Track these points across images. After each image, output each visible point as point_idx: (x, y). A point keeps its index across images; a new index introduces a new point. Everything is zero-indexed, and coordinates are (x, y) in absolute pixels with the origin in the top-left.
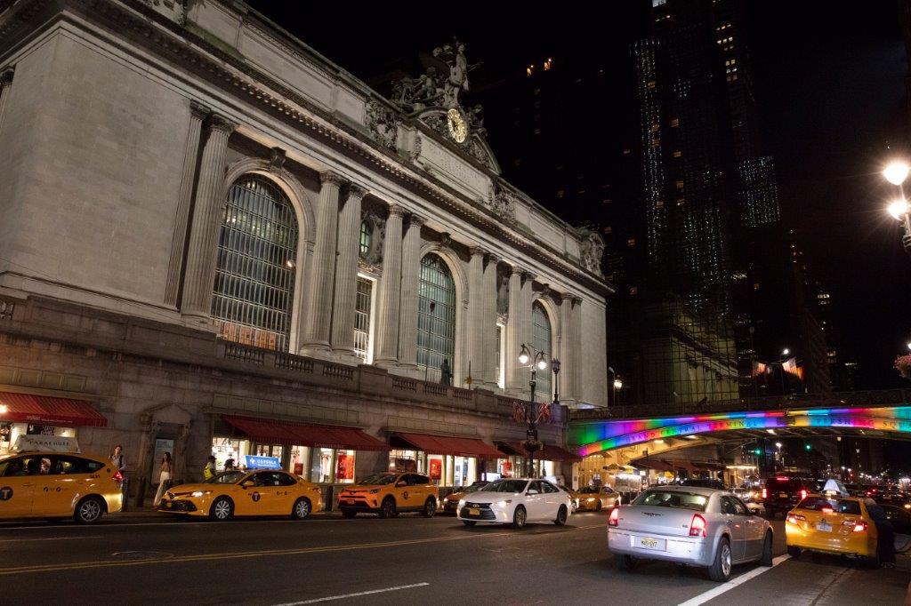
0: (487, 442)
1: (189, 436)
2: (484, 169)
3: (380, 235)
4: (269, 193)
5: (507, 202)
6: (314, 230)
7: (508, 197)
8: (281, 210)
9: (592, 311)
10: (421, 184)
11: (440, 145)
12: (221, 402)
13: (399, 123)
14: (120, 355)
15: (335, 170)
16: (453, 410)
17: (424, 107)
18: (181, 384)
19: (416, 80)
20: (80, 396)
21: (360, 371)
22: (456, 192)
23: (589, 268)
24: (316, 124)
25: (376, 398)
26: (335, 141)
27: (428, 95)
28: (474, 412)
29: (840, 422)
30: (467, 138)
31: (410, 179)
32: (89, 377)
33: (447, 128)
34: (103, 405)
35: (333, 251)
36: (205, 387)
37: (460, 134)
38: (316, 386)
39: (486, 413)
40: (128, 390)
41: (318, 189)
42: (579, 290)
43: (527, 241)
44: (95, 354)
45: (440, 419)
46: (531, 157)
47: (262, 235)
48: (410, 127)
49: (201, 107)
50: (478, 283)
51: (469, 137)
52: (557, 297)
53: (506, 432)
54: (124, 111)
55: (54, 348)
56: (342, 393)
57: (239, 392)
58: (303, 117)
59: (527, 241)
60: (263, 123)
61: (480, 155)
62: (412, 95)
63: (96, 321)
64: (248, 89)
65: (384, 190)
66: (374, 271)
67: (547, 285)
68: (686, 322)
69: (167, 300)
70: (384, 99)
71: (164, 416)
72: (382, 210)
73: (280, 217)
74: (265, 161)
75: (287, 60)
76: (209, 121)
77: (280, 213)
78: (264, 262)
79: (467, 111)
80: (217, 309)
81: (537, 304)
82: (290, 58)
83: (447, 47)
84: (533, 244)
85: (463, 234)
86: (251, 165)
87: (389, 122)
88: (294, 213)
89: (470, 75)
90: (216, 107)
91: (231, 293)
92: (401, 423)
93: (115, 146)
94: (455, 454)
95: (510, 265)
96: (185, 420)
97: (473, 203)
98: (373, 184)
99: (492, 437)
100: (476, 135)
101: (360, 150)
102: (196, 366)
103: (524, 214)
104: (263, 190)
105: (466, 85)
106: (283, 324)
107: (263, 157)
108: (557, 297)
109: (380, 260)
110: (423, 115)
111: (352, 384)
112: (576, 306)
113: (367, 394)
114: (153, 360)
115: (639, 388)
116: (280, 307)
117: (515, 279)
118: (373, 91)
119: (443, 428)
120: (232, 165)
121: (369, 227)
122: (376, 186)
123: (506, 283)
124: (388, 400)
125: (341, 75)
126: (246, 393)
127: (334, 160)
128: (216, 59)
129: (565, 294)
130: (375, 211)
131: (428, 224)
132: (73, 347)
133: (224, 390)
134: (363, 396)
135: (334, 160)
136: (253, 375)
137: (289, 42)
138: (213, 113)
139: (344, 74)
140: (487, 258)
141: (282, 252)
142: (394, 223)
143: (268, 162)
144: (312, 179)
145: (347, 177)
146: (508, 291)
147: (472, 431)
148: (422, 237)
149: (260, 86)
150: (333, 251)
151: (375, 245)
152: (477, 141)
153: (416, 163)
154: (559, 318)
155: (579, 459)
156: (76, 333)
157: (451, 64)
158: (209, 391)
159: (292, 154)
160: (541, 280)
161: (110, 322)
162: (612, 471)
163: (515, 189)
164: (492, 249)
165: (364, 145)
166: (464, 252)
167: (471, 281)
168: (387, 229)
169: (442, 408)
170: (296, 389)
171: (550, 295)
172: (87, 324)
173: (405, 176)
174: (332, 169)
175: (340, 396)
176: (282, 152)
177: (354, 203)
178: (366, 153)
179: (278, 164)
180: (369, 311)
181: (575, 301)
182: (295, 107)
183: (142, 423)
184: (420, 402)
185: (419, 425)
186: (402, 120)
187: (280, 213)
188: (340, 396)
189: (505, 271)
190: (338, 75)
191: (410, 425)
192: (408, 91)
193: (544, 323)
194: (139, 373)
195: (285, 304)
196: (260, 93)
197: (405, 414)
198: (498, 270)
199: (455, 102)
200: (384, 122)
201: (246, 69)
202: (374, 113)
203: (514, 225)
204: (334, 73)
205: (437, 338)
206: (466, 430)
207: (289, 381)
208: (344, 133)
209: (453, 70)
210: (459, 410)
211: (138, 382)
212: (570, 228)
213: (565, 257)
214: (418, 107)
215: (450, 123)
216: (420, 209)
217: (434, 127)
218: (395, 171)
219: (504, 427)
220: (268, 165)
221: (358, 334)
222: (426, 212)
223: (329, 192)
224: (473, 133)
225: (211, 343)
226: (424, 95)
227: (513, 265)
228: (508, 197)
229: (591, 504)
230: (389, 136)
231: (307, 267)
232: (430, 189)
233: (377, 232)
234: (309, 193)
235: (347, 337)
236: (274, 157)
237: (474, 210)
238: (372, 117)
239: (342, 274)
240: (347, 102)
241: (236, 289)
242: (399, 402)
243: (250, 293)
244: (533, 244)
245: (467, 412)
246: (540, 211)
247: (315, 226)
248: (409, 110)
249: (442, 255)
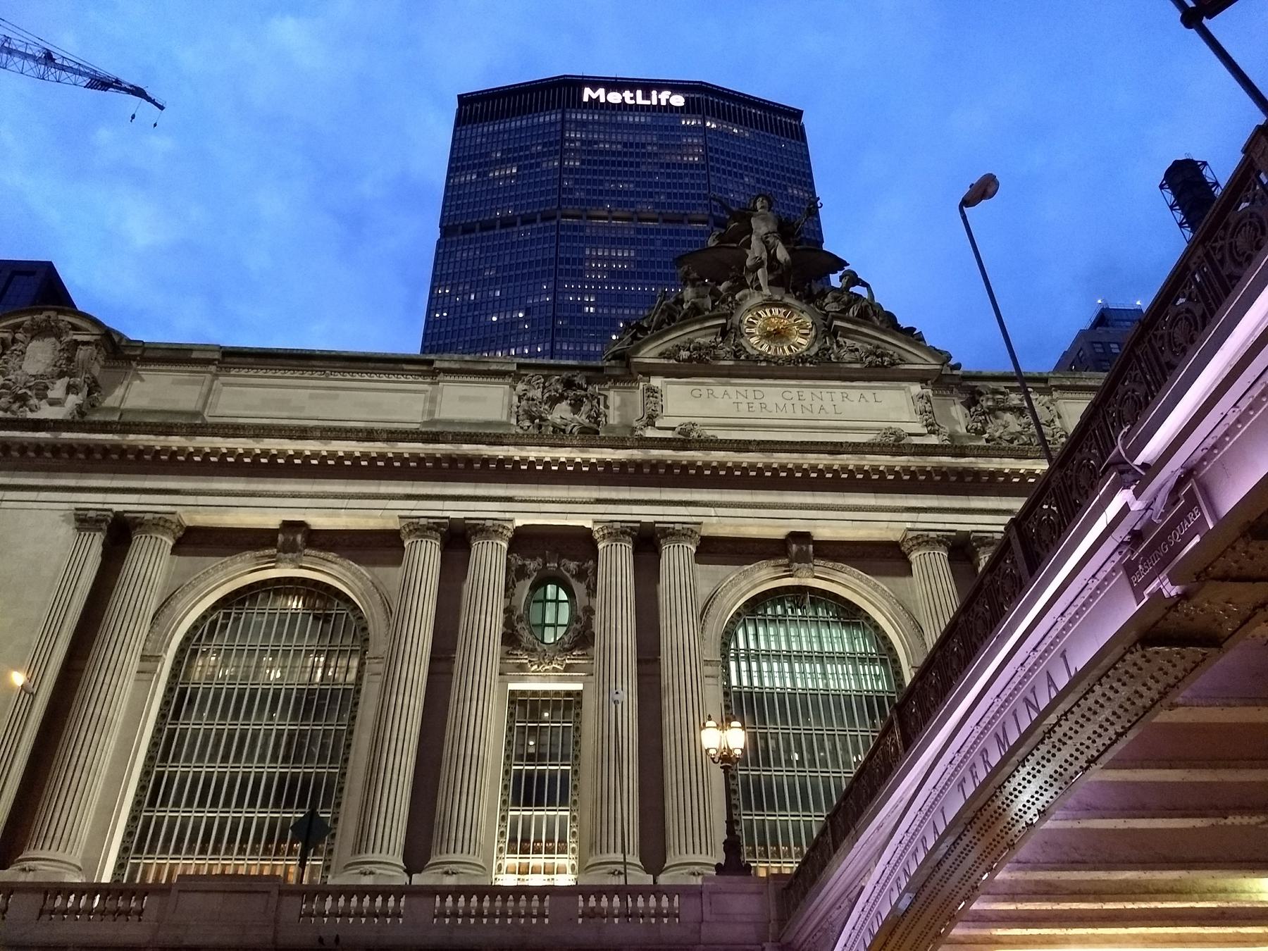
48: (636, 381)
49: (92, 514)
72: (579, 544)
76: (119, 534)
101: (469, 460)
125: (437, 364)
128: (109, 436)
137: (314, 363)
153: (650, 433)
165: (467, 448)
173: (608, 464)
178: (486, 461)
186: (616, 379)
196: (215, 452)
200: (561, 398)
204: (425, 368)
236: (297, 538)
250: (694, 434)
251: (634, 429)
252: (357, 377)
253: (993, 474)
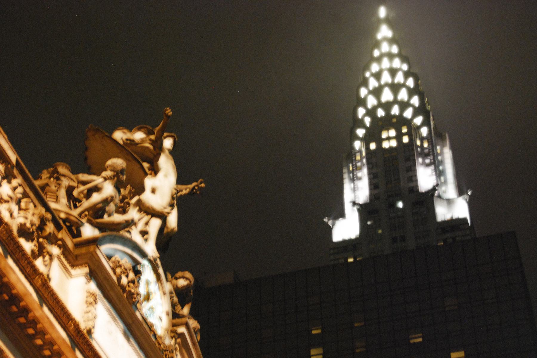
48: (73, 266)
83: (139, 136)
100: (182, 330)
105: (173, 220)
199: (150, 248)
209: (149, 182)
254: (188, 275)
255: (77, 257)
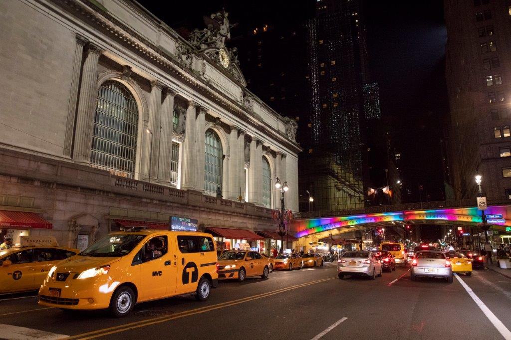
0: (252, 231)
1: (98, 233)
2: (238, 83)
3: (183, 118)
4: (122, 92)
5: (249, 102)
6: (148, 114)
7: (250, 99)
8: (128, 102)
9: (291, 161)
10: (206, 90)
11: (216, 69)
12: (114, 212)
13: (193, 55)
14: (55, 186)
15: (160, 80)
16: (235, 214)
17: (207, 47)
18: (91, 202)
19: (202, 31)
20: (33, 211)
21: (188, 193)
22: (224, 95)
23: (290, 138)
24: (149, 53)
25: (198, 208)
26: (159, 63)
27: (209, 40)
28: (245, 215)
29: (430, 216)
30: (229, 65)
31: (200, 87)
32: (34, 198)
33: (219, 59)
34: (45, 215)
35: (157, 125)
36: (105, 203)
37: (225, 63)
38: (166, 202)
39: (252, 215)
40: (60, 206)
41: (150, 91)
42: (285, 150)
43: (260, 123)
44: (39, 184)
45: (229, 219)
46: (267, 78)
47: (118, 116)
49: (82, 38)
50: (235, 146)
51: (230, 65)
52: (274, 154)
53: (262, 226)
54: (35, 37)
55: (14, 180)
56: (180, 206)
57: (124, 206)
58: (142, 48)
59: (260, 123)
60: (119, 50)
61: (236, 75)
62: (200, 40)
63: (39, 163)
64: (111, 29)
65: (185, 92)
66: (180, 138)
67: (269, 147)
68: (336, 168)
69: (65, 153)
70: (186, 41)
71: (82, 221)
73: (128, 106)
74: (119, 73)
75: (131, 14)
77: (128, 104)
78: (120, 132)
79: (229, 50)
80: (93, 158)
81: (264, 157)
82: (133, 13)
83: (219, 14)
84: (263, 125)
85: (227, 118)
86: (112, 75)
87: (188, 53)
88: (136, 104)
89: (232, 31)
90: (92, 39)
91: (105, 151)
92: (210, 222)
93: (30, 58)
94: (236, 239)
95: (251, 136)
96: (95, 223)
97: (233, 102)
98: (180, 89)
99: (255, 228)
101: (173, 69)
102: (100, 191)
103: (257, 108)
104: (118, 90)
105: (229, 36)
106: (131, 168)
107: (118, 70)
108: (274, 154)
109: (184, 132)
110: (206, 51)
111: (185, 201)
112: (283, 158)
113: (193, 206)
114: (74, 187)
115: (314, 202)
116: (129, 158)
117: (253, 144)
118: (180, 36)
119: (231, 224)
120: (101, 75)
121: (177, 113)
122: (182, 90)
123: (249, 146)
124: (203, 209)
125: (162, 25)
126: (128, 206)
127: (159, 74)
129: (278, 152)
130: (181, 104)
131: (208, 112)
132: (25, 179)
133: (116, 205)
134: (190, 207)
135: (159, 74)
136: (133, 196)
138: (89, 42)
139: (163, 25)
140: (240, 132)
141: (130, 128)
142: (191, 111)
143: (122, 73)
144: (146, 85)
145: (166, 84)
146: (249, 150)
147: (245, 226)
148: (206, 120)
149: (117, 28)
150: (157, 125)
151: (180, 124)
152: (235, 67)
153: (202, 78)
154: (275, 165)
155: (296, 239)
156: (27, 171)
157: (221, 23)
158: (107, 206)
159: (135, 70)
160: (266, 144)
161: (47, 164)
162: (314, 245)
163: (254, 95)
164: (243, 128)
165: (176, 67)
166: (228, 128)
167: (231, 144)
168: (187, 114)
169: (230, 214)
170: (155, 204)
171: (271, 153)
172: (33, 165)
173: (197, 85)
174: (157, 79)
175: (179, 207)
176: (129, 68)
177: (170, 99)
178: (177, 71)
179: (127, 75)
180: (178, 160)
181: (283, 156)
182: (138, 42)
183: (70, 226)
184: (219, 210)
185: (218, 223)
187: (128, 104)
188: (179, 207)
189: (248, 139)
190: (161, 25)
191: (214, 223)
192: (198, 37)
193: (267, 168)
194: (66, 196)
195: (132, 156)
196: (117, 32)
197: (212, 217)
198: (245, 139)
199: (223, 45)
201: (110, 18)
202: (180, 49)
203: (253, 114)
204: (158, 24)
205: (214, 176)
206: (241, 225)
207: (152, 199)
208: (165, 59)
209: (222, 27)
210: (240, 215)
211: (66, 201)
212: (280, 117)
213: (278, 132)
214: (203, 47)
215: (220, 57)
216: (205, 104)
217: (213, 58)
218: (192, 82)
219: (260, 223)
220: (121, 75)
221: (173, 173)
222: (209, 106)
223: (156, 92)
224: (232, 63)
225: (107, 177)
226: (206, 40)
227: (252, 136)
228: (250, 99)
229: (311, 263)
230: (188, 62)
231: (144, 132)
232: (210, 93)
233: (181, 116)
234: (144, 92)
235: (167, 174)
237: (233, 105)
238: (179, 50)
239: (164, 138)
240: (165, 41)
241: (103, 147)
242: (209, 210)
243: (112, 150)
244: (263, 125)
245: (242, 215)
246: (265, 107)
247: (148, 111)
248: (198, 48)
249: (216, 130)
250: (210, 83)
251: (200, 75)
252: (141, 16)
253: (248, 118)
254: (236, 48)
255: (199, 55)
